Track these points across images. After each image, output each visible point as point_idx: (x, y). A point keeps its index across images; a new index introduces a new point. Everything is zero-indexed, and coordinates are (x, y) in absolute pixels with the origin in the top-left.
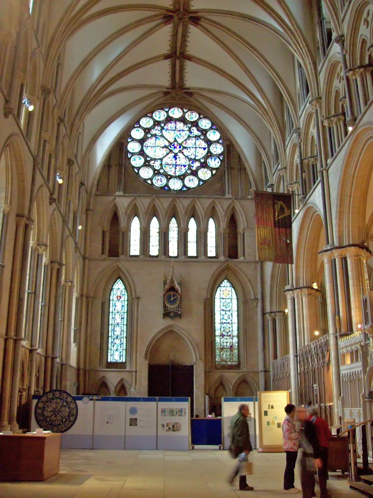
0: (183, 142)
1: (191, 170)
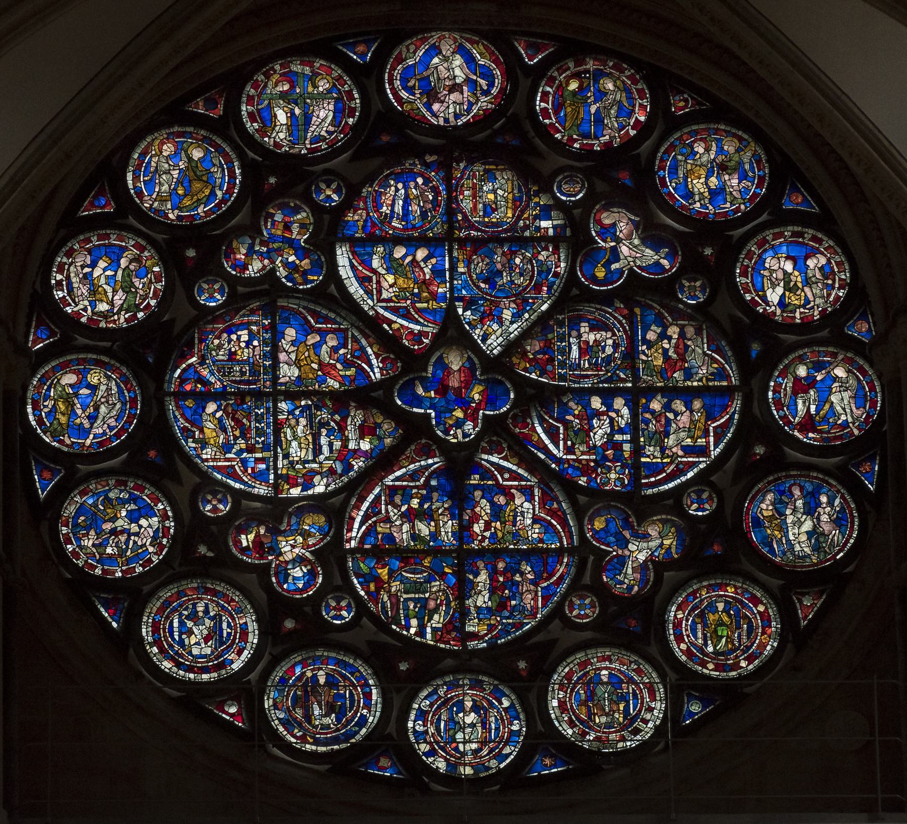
0: (513, 347)
1: (602, 593)
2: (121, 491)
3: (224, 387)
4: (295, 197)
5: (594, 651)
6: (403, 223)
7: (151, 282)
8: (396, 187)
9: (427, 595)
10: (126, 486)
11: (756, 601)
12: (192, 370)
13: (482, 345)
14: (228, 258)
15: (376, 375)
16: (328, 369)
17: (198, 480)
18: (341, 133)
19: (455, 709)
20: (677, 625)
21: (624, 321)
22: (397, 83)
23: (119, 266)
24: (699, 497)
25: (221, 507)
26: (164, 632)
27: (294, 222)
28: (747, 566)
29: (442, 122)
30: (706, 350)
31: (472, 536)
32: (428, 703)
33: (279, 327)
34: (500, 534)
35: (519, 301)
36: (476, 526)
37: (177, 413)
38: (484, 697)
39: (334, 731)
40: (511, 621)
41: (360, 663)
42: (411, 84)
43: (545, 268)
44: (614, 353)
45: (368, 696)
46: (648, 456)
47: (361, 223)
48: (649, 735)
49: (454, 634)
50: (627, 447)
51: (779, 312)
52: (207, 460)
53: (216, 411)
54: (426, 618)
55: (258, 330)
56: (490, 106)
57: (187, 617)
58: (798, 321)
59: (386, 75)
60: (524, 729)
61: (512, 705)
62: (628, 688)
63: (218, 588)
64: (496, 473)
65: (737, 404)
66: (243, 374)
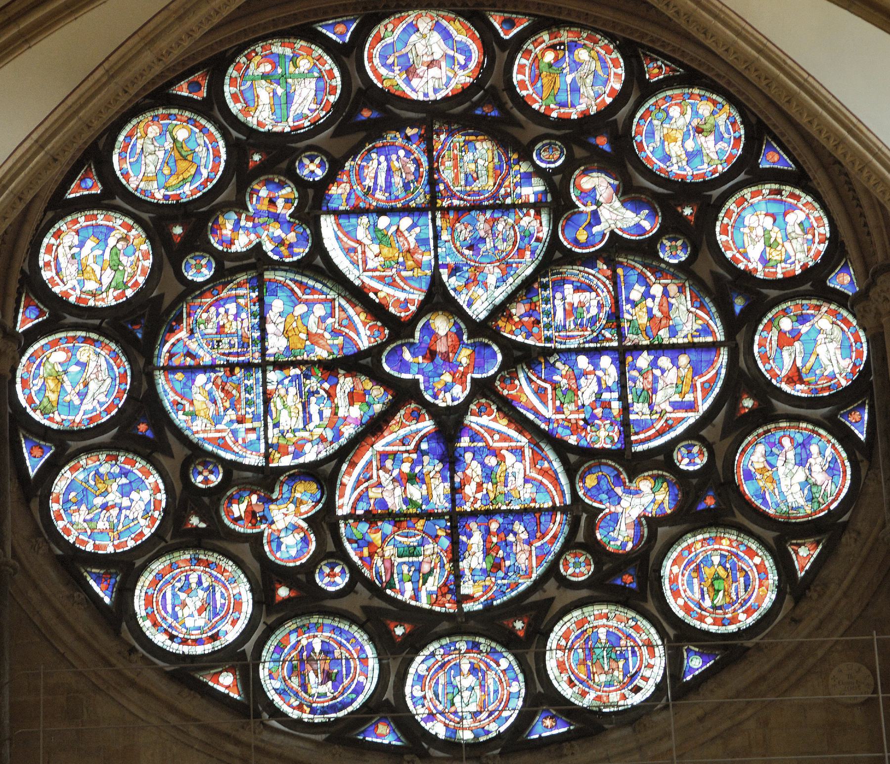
0: (500, 310)
2: (112, 466)
3: (213, 359)
4: (279, 173)
5: (590, 608)
6: (387, 194)
7: (138, 259)
9: (421, 558)
10: (117, 460)
12: (180, 344)
13: (467, 310)
15: (364, 344)
17: (189, 452)
19: (452, 672)
20: (673, 580)
22: (376, 61)
24: (689, 452)
25: (212, 477)
26: (157, 605)
27: (278, 197)
28: (740, 519)
30: (689, 306)
31: (465, 499)
33: (267, 299)
34: (492, 496)
36: (467, 487)
37: (166, 387)
39: (332, 699)
42: (390, 61)
43: (527, 233)
44: (599, 313)
45: (364, 661)
47: (345, 196)
49: (449, 597)
50: (616, 406)
51: (760, 267)
52: (197, 432)
58: (780, 276)
61: (510, 666)
63: (211, 559)
64: (486, 435)
65: (723, 357)
66: (232, 346)
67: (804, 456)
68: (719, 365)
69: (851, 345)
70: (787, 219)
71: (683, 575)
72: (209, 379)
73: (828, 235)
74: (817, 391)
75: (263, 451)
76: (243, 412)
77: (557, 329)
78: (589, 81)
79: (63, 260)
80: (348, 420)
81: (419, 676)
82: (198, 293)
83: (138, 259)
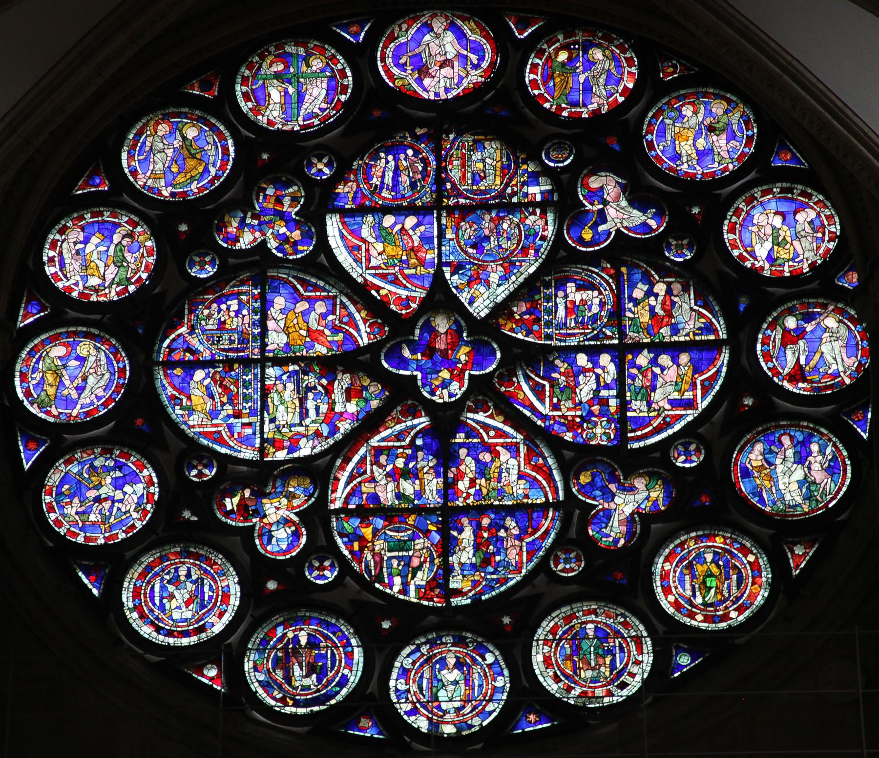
0: (501, 310)
2: (107, 459)
3: (213, 355)
5: (579, 605)
6: (393, 193)
8: (386, 159)
9: (411, 553)
10: (112, 454)
11: (745, 551)
12: (181, 340)
13: (469, 308)
14: (219, 231)
15: (364, 340)
16: (316, 335)
17: (184, 446)
18: (333, 109)
19: (438, 666)
20: (665, 577)
21: (611, 281)
22: (389, 61)
23: (112, 242)
25: (206, 471)
27: (286, 195)
29: (432, 97)
30: (693, 305)
31: (457, 494)
32: (410, 661)
33: (269, 296)
34: (485, 491)
35: (506, 265)
37: (165, 382)
38: (467, 654)
39: (315, 692)
40: (494, 577)
41: (342, 622)
42: (402, 61)
44: (601, 311)
45: (349, 656)
46: (635, 411)
47: (351, 195)
48: (636, 689)
49: (437, 591)
50: (613, 402)
51: (767, 266)
52: (193, 426)
53: (204, 379)
54: (410, 575)
55: (248, 300)
56: (480, 79)
57: (169, 582)
58: (787, 274)
59: (379, 53)
60: (508, 685)
61: (496, 661)
62: (614, 642)
63: (201, 552)
64: (481, 431)
65: (725, 357)
66: (232, 342)
67: (804, 454)
68: (720, 363)
69: (857, 344)
70: (798, 217)
71: (675, 572)
72: (207, 375)
73: (838, 234)
74: (819, 389)
75: (257, 445)
76: (240, 407)
77: (559, 327)
78: (602, 80)
79: (66, 255)
80: (345, 415)
81: (404, 669)
82: (201, 289)
83: (143, 254)
